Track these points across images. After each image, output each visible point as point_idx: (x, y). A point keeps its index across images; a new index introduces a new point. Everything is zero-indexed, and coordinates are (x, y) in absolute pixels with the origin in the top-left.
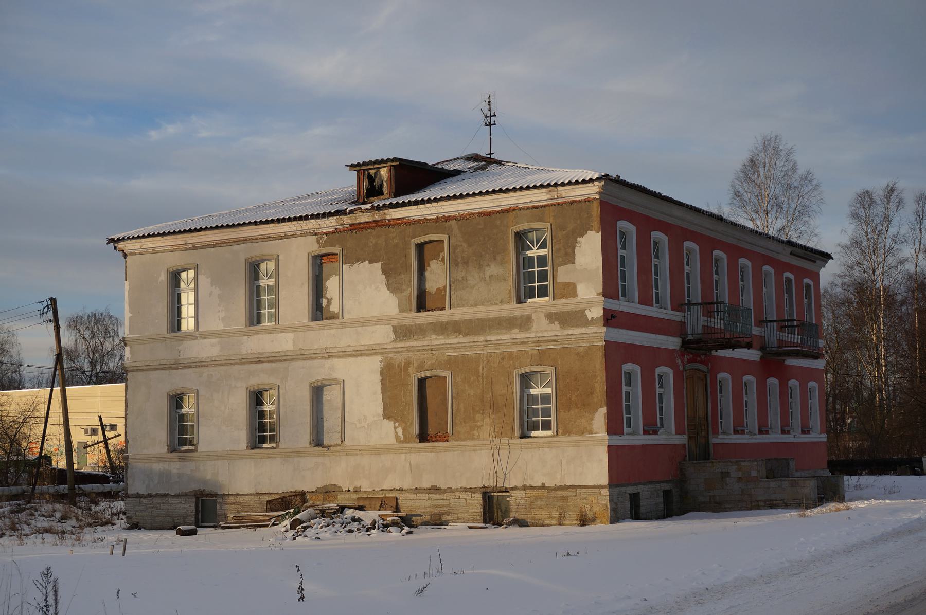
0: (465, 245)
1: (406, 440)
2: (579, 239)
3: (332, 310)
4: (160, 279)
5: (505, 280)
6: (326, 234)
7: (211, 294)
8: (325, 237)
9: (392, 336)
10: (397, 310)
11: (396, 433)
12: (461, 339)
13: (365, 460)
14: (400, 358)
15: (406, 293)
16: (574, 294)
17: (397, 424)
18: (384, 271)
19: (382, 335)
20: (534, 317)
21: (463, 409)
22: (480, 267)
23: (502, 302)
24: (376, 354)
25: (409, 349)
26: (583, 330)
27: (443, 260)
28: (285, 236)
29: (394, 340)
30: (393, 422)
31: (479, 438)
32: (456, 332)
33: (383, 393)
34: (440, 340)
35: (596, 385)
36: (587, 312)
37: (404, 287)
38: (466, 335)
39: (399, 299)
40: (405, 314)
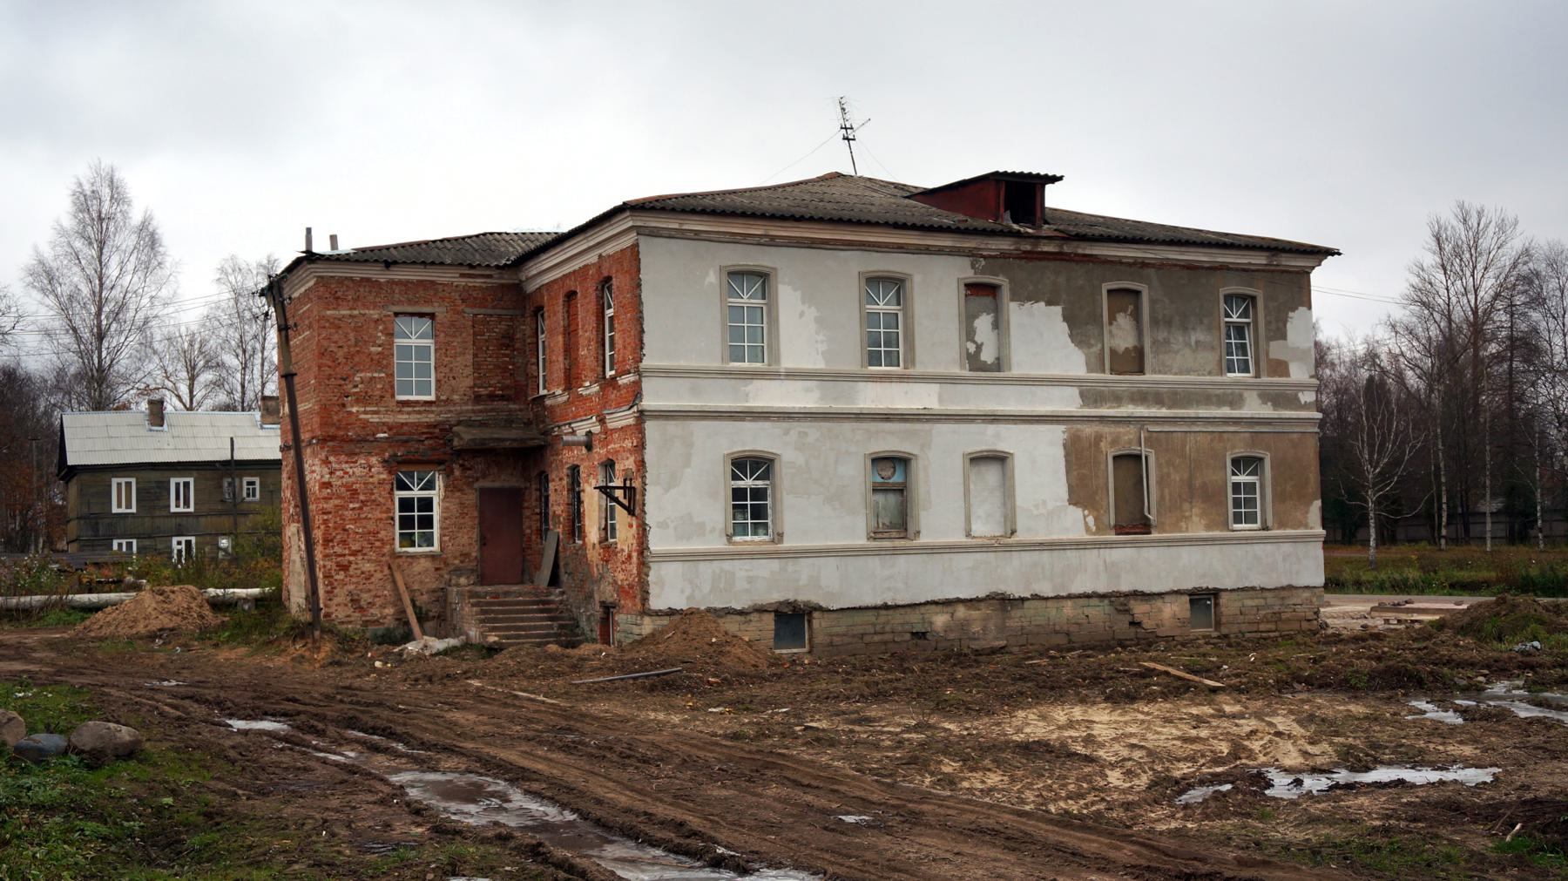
0: (1167, 301)
1: (1099, 530)
2: (1291, 314)
6: (985, 257)
7: (802, 314)
8: (983, 263)
11: (1086, 523)
12: (1164, 412)
13: (1045, 557)
14: (1088, 430)
15: (1091, 350)
16: (1287, 374)
17: (1086, 512)
18: (1066, 318)
20: (1246, 394)
21: (1167, 498)
23: (1210, 373)
25: (1102, 419)
29: (1082, 407)
31: (1187, 530)
32: (1157, 403)
33: (1067, 472)
35: (1311, 475)
36: (1300, 394)
37: (1092, 341)
38: (1170, 408)
39: (1086, 355)
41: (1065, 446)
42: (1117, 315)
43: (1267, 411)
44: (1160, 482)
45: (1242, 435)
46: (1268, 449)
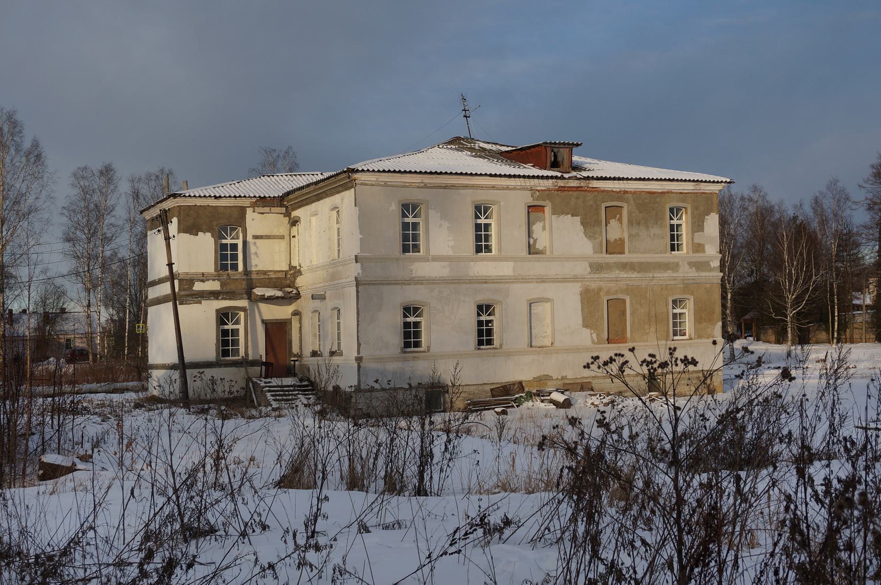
1: (599, 343)
3: (537, 247)
4: (391, 208)
5: (663, 238)
8: (538, 193)
9: (589, 270)
10: (592, 252)
14: (594, 286)
15: (597, 240)
16: (704, 251)
18: (582, 223)
19: (583, 269)
22: (648, 227)
23: (661, 252)
24: (577, 282)
25: (601, 280)
26: (707, 274)
27: (620, 220)
28: (507, 188)
29: (590, 273)
30: (589, 330)
31: (647, 341)
32: (631, 270)
33: (582, 310)
34: (623, 275)
36: (711, 262)
37: (596, 236)
38: (639, 272)
40: (597, 255)
41: (581, 294)
42: (610, 221)
43: (693, 273)
44: (632, 314)
45: (679, 286)
46: (692, 293)
